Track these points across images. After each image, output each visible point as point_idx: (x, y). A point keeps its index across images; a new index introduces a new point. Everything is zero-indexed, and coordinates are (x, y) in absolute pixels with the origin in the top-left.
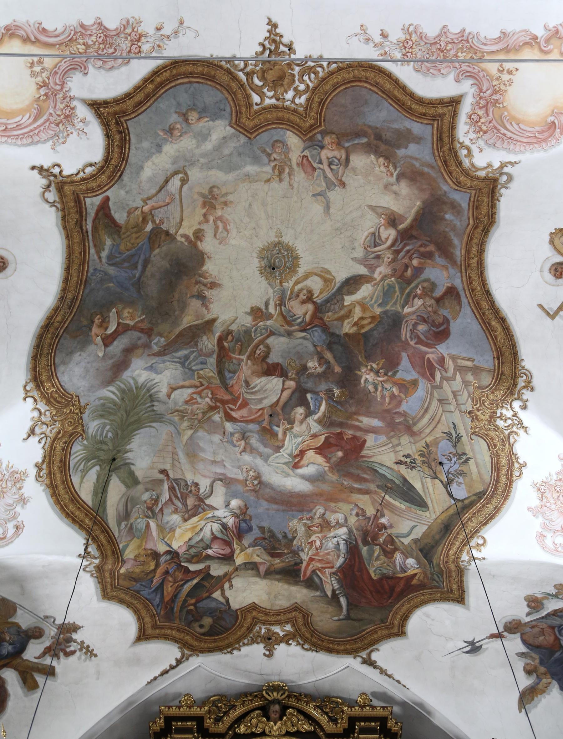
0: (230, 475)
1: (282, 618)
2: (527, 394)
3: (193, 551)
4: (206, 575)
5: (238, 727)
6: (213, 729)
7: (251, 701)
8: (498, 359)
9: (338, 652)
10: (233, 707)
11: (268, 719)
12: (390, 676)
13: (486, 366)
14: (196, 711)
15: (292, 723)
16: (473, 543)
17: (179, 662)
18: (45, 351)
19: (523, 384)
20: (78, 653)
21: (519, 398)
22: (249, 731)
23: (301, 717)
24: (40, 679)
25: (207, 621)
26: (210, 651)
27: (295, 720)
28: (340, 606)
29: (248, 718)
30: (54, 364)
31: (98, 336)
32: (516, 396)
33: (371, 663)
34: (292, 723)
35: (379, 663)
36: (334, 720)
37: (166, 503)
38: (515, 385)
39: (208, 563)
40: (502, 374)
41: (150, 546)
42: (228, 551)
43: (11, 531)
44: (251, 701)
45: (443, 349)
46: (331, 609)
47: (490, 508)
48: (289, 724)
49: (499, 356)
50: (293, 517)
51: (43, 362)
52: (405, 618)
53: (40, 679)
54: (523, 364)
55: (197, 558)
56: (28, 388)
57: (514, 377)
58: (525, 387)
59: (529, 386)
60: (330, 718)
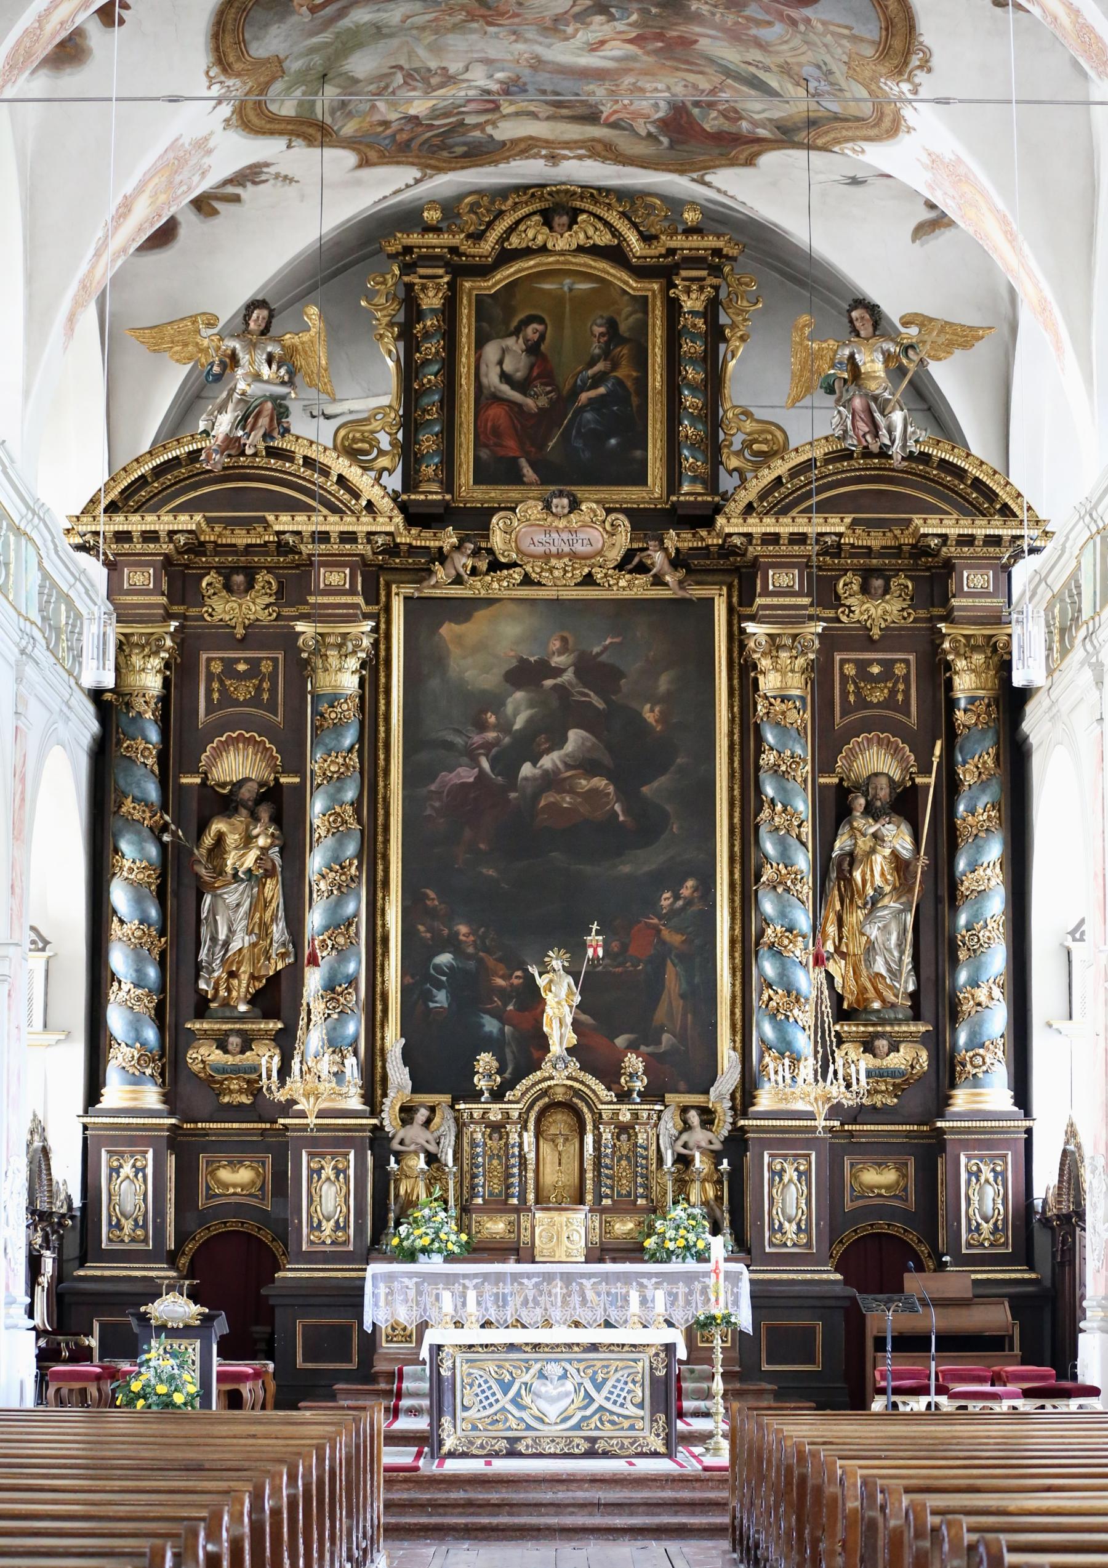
0: (492, 57)
1: (572, 145)
2: (920, 77)
3: (437, 113)
4: (461, 123)
5: (508, 239)
6: (473, 251)
7: (526, 203)
8: (887, 29)
9: (655, 169)
10: (500, 214)
11: (551, 229)
12: (731, 197)
13: (868, 36)
14: (446, 239)
15: (586, 233)
16: (850, 145)
17: (418, 181)
18: (230, 27)
19: (918, 63)
20: (272, 182)
21: (909, 80)
22: (524, 245)
23: (600, 225)
24: (217, 205)
25: (460, 150)
26: (463, 168)
27: (591, 231)
28: (661, 143)
29: (522, 227)
30: (244, 41)
31: (302, 6)
32: (906, 77)
33: (708, 185)
34: (586, 233)
35: (715, 184)
36: (647, 238)
37: (399, 87)
38: (906, 63)
39: (461, 117)
40: (890, 47)
41: (377, 118)
42: (492, 106)
43: (196, 179)
44: (526, 203)
45: (808, 12)
46: (644, 142)
47: (872, 132)
48: (582, 236)
49: (889, 26)
50: (590, 83)
51: (229, 39)
52: (758, 154)
53: (217, 205)
54: (921, 39)
55: (446, 115)
56: (212, 74)
57: (907, 53)
58: (920, 67)
59: (925, 66)
60: (640, 233)
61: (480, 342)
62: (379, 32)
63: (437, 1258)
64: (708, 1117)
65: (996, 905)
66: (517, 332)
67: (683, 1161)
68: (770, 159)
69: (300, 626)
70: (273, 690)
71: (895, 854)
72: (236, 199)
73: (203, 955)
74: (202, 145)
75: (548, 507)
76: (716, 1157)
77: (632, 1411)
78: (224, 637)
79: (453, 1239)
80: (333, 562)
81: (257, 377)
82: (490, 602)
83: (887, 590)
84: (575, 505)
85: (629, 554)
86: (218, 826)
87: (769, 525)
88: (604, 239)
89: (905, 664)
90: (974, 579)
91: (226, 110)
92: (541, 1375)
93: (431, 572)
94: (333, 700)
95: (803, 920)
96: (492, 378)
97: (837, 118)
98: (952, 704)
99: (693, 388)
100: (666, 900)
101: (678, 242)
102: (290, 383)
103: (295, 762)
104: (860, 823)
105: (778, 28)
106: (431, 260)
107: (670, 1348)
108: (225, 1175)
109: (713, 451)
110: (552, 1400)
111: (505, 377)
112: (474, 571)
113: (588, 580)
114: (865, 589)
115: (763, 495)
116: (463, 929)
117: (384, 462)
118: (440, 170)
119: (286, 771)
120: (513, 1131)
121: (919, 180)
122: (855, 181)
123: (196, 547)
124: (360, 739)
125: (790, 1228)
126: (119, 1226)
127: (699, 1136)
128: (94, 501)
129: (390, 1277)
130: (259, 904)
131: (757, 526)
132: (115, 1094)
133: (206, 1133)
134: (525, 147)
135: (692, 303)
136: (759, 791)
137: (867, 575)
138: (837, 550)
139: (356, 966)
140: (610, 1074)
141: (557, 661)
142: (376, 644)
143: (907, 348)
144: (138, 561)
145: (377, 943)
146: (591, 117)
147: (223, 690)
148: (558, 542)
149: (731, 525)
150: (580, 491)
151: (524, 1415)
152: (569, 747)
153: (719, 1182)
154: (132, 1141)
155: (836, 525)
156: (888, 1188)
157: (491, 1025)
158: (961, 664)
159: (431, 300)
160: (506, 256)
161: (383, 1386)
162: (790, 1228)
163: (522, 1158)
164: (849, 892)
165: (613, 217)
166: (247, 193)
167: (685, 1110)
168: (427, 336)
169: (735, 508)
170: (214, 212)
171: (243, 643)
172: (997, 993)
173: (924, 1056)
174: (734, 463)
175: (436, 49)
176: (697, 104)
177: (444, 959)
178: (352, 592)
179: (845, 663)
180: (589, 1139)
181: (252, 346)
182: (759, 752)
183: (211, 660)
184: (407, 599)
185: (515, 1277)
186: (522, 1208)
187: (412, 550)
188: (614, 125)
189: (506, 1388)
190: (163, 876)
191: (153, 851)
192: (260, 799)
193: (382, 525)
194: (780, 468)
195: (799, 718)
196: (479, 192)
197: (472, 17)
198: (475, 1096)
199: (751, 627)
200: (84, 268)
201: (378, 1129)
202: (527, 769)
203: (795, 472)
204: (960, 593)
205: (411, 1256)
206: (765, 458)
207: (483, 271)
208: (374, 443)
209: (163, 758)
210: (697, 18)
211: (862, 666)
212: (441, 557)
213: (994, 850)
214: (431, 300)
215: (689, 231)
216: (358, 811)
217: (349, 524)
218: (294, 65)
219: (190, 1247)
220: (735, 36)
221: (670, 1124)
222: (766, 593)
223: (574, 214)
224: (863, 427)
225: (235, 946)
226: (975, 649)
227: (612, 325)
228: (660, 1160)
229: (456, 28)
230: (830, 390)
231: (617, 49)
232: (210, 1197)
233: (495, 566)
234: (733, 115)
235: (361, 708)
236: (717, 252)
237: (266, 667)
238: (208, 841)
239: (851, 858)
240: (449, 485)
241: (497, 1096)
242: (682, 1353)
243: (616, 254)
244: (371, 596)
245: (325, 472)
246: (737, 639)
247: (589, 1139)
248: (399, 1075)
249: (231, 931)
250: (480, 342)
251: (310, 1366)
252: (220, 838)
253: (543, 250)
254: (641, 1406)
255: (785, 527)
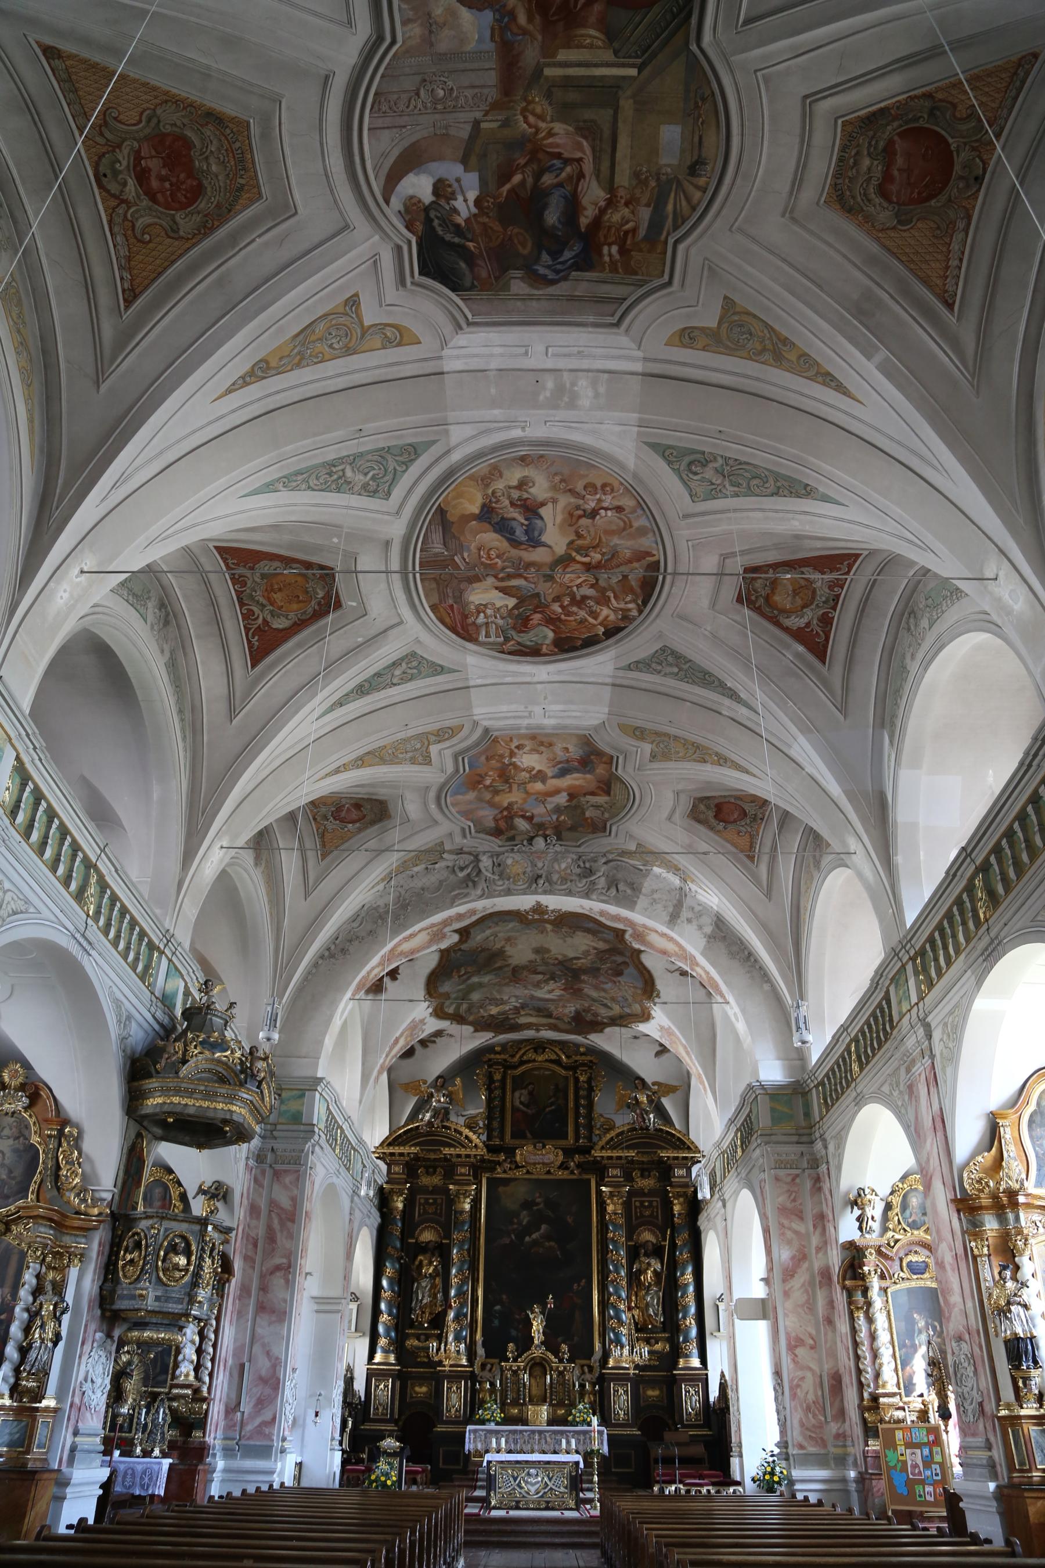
4: (507, 1018)
10: (520, 1049)
14: (503, 1056)
36: (567, 1057)
61: (513, 1092)
62: (481, 985)
63: (493, 1424)
64: (591, 1369)
65: (691, 1289)
66: (525, 1088)
67: (582, 1386)
68: (608, 1030)
69: (451, 1187)
70: (441, 1209)
71: (655, 1271)
72: (434, 1042)
73: (413, 1304)
74: (422, 1022)
75: (535, 1147)
76: (593, 1385)
77: (562, 1489)
78: (425, 1190)
79: (499, 1416)
80: (463, 1165)
81: (439, 1101)
82: (516, 1179)
83: (649, 1176)
84: (544, 1147)
85: (563, 1163)
86: (420, 1257)
87: (609, 1153)
88: (554, 1057)
89: (656, 1201)
90: (679, 1172)
91: (430, 1010)
92: (529, 1474)
93: (496, 1169)
94: (462, 1212)
95: (624, 1295)
96: (517, 1103)
97: (629, 1015)
98: (673, 1215)
99: (583, 1106)
100: (575, 1286)
101: (578, 1058)
102: (450, 1104)
103: (448, 1236)
104: (643, 1259)
105: (610, 985)
106: (498, 1063)
107: (577, 1463)
108: (417, 1389)
109: (590, 1128)
110: (533, 1485)
111: (521, 1103)
112: (510, 1169)
113: (549, 1172)
114: (642, 1176)
115: (608, 1143)
116: (504, 1297)
117: (481, 1131)
118: (501, 1034)
119: (445, 1238)
120: (521, 1373)
121: (656, 1035)
122: (635, 1037)
123: (416, 1158)
124: (470, 1227)
125: (622, 1413)
126: (377, 1409)
127: (588, 1376)
128: (383, 1142)
129: (475, 1431)
130: (434, 1286)
131: (605, 1154)
132: (378, 1357)
133: (411, 1372)
134: (528, 1026)
135: (582, 1079)
136: (608, 1247)
137: (642, 1171)
138: (632, 1162)
139: (467, 1310)
140: (556, 1352)
141: (538, 1200)
142: (476, 1194)
143: (654, 1093)
144: (397, 1164)
145: (474, 1301)
146: (550, 1016)
147: (424, 1209)
148: (538, 1159)
149: (597, 1153)
150: (546, 1142)
151: (522, 1491)
152: (542, 1231)
153: (595, 1395)
154: (384, 1375)
155: (632, 1153)
156: (657, 1397)
157: (514, 1333)
158: (676, 1202)
159: (497, 1077)
160: (522, 1063)
161: (471, 1476)
162: (622, 1413)
163: (524, 1384)
164: (640, 1284)
165: (557, 1050)
166: (438, 1040)
167: (582, 1366)
168: (496, 1088)
169: (598, 1147)
170: (427, 1046)
171: (432, 1193)
172: (693, 1322)
173: (667, 1347)
174: (597, 1132)
175: (499, 992)
176: (584, 1011)
177: (498, 1308)
178: (469, 1175)
179: (636, 1202)
180: (548, 1377)
181: (438, 1091)
182: (607, 1233)
183: (421, 1198)
184: (488, 1178)
185: (521, 1432)
186: (524, 1404)
187: (490, 1161)
188: (557, 1019)
189: (515, 1479)
190: (400, 1275)
191: (397, 1266)
192: (435, 1248)
193: (479, 1152)
194: (613, 1134)
195: (621, 1221)
196: (513, 1041)
197: (511, 981)
198: (507, 1360)
199: (604, 1189)
200: (381, 1061)
201: (473, 1372)
202: (527, 1239)
203: (618, 1135)
204: (674, 1177)
205: (483, 1422)
206: (608, 1130)
207: (515, 1067)
208: (478, 1124)
209: (402, 1233)
210: (583, 982)
211: (642, 1202)
212: (499, 1163)
213: (690, 1269)
214: (497, 1077)
215: (582, 1054)
216: (469, 1253)
217: (468, 1152)
218: (453, 996)
219: (403, 1417)
220: (596, 988)
221: (577, 1372)
222: (608, 1177)
223: (544, 1049)
224: (640, 1120)
225: (425, 1301)
226: (681, 1196)
227: (557, 1086)
228: (574, 1386)
229: (507, 984)
230: (629, 1107)
231: (558, 993)
232: (412, 1397)
233: (517, 1167)
234: (596, 1015)
235: (471, 1216)
236: (591, 1061)
237: (439, 1201)
238: (417, 1263)
239: (640, 1272)
240: (502, 1139)
241: (515, 1360)
242: (582, 1465)
243: (558, 1062)
244: (475, 1176)
245: (461, 1133)
246: (599, 1193)
247: (548, 1377)
248: (481, 1351)
249: (423, 1297)
250: (513, 1092)
251: (446, 1467)
252: (421, 1261)
253: (534, 1061)
254: (566, 1488)
255: (615, 1154)
